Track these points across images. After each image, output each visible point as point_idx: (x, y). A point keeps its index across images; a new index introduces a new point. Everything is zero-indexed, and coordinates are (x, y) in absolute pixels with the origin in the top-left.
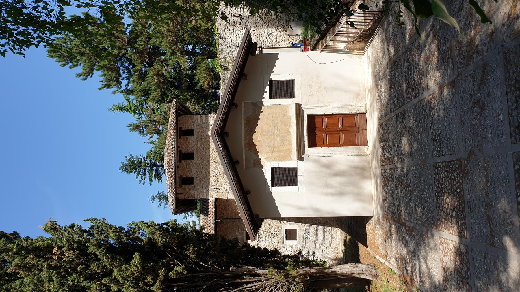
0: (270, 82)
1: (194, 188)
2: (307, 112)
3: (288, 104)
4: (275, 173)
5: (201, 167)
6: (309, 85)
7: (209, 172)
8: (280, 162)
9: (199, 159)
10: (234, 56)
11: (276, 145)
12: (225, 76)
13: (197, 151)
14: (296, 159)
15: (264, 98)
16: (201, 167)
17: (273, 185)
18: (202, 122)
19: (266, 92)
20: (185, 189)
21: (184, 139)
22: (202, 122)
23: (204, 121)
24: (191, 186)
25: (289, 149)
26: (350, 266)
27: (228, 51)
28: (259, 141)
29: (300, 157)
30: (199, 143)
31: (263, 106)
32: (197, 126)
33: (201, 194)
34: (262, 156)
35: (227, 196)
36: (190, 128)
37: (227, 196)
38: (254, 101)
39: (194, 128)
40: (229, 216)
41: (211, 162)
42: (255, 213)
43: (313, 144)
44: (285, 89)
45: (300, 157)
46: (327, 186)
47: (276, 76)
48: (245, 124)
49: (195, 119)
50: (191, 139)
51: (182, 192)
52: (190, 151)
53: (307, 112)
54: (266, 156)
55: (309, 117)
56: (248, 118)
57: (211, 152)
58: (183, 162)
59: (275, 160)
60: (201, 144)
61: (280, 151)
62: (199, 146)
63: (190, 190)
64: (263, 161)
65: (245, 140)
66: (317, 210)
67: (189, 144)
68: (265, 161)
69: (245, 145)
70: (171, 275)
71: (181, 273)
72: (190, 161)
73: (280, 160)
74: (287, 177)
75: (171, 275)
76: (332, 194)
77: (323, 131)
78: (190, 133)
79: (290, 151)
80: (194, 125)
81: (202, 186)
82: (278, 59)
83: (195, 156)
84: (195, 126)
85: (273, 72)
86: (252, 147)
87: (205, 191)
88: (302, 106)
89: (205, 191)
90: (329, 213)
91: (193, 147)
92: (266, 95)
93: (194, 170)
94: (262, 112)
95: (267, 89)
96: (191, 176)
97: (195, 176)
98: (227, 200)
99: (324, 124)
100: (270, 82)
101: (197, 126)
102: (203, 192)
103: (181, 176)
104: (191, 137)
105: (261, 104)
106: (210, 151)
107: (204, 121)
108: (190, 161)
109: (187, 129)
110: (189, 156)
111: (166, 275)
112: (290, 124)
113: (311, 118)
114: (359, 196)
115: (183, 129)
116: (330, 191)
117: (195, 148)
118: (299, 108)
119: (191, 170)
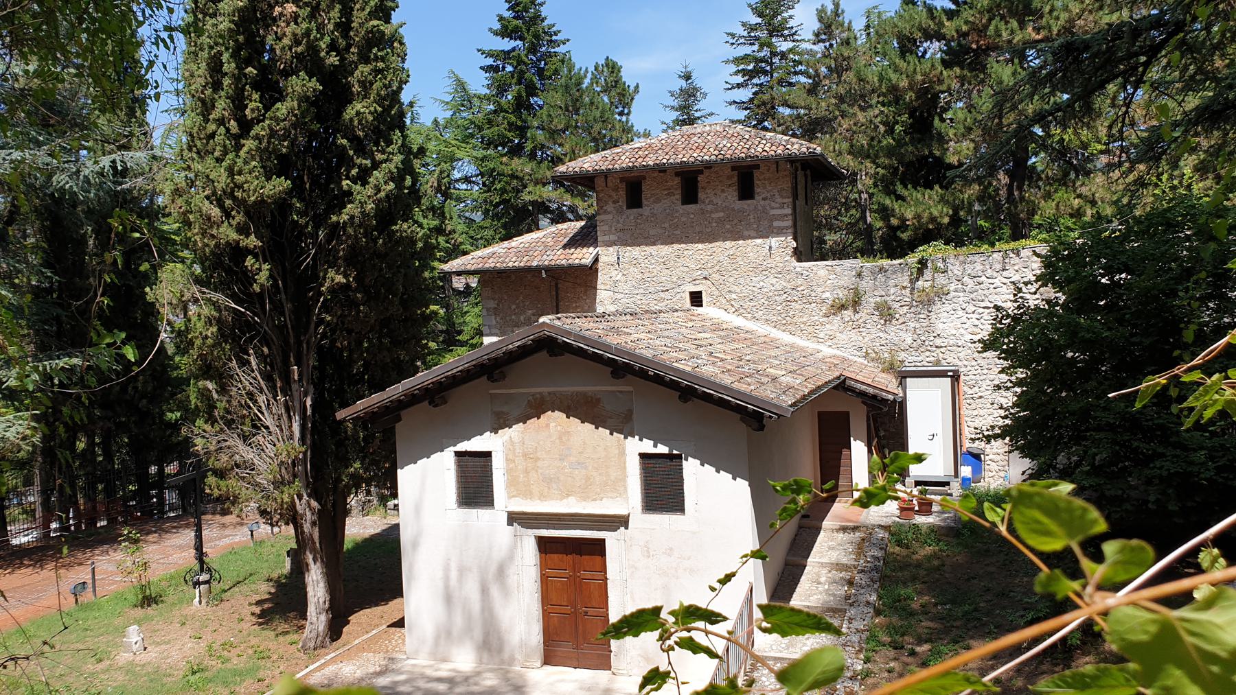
0: (679, 457)
1: (619, 212)
2: (612, 540)
3: (630, 499)
4: (482, 459)
5: (666, 225)
6: (671, 549)
7: (654, 244)
8: (502, 471)
9: (684, 219)
10: (952, 294)
11: (540, 464)
12: (895, 272)
13: (703, 212)
14: (511, 509)
15: (641, 440)
16: (666, 225)
17: (458, 454)
18: (773, 218)
19: (655, 446)
20: (616, 189)
21: (729, 178)
22: (773, 218)
23: (776, 224)
24: (622, 203)
25: (531, 493)
26: (321, 600)
27: (966, 279)
28: (548, 425)
29: (513, 518)
30: (722, 214)
31: (626, 438)
32: (764, 207)
33: (606, 228)
34: (515, 432)
35: (603, 287)
36: (757, 190)
37: (603, 287)
38: (635, 416)
39: (758, 202)
40: (562, 294)
41: (676, 246)
42: (404, 413)
43: (545, 545)
44: (663, 492)
45: (514, 518)
46: (462, 571)
47: (691, 467)
48: (584, 394)
49: (780, 200)
50: (732, 195)
51: (610, 184)
52: (701, 195)
53: (612, 540)
54: (516, 440)
55: (601, 542)
56: (598, 400)
57: (700, 246)
58: (677, 180)
59: (507, 460)
60: (720, 221)
61: (526, 472)
62: (714, 216)
63: (614, 202)
64: (506, 433)
65: (549, 393)
66: (415, 545)
67: (719, 192)
68: (506, 438)
69: (540, 393)
70: (249, 261)
71: (255, 281)
72: (678, 196)
73: (509, 471)
74: (475, 486)
75: (249, 261)
76: (447, 578)
77: (574, 572)
78: (746, 192)
79: (527, 494)
80: (764, 199)
81: (622, 230)
82: (734, 479)
83: (691, 208)
84: (762, 203)
85: (702, 464)
86: (536, 409)
87: (613, 238)
88: (622, 529)
89: (613, 238)
90: (410, 570)
91: (711, 202)
92: (648, 446)
93: (658, 208)
94: (611, 434)
95: (663, 449)
96: (645, 202)
97: (645, 211)
98: (596, 288)
99: (588, 575)
100: (679, 457)
101: (764, 207)
102: (610, 232)
103: (644, 178)
104: (736, 194)
105: (629, 434)
106: (703, 242)
107: (776, 224)
108: (678, 197)
109: (756, 182)
110: (690, 195)
111: (248, 251)
112: (585, 498)
113: (598, 547)
114: (445, 635)
115: (756, 174)
116: (454, 574)
117: (710, 207)
118: (620, 522)
119: (658, 200)
